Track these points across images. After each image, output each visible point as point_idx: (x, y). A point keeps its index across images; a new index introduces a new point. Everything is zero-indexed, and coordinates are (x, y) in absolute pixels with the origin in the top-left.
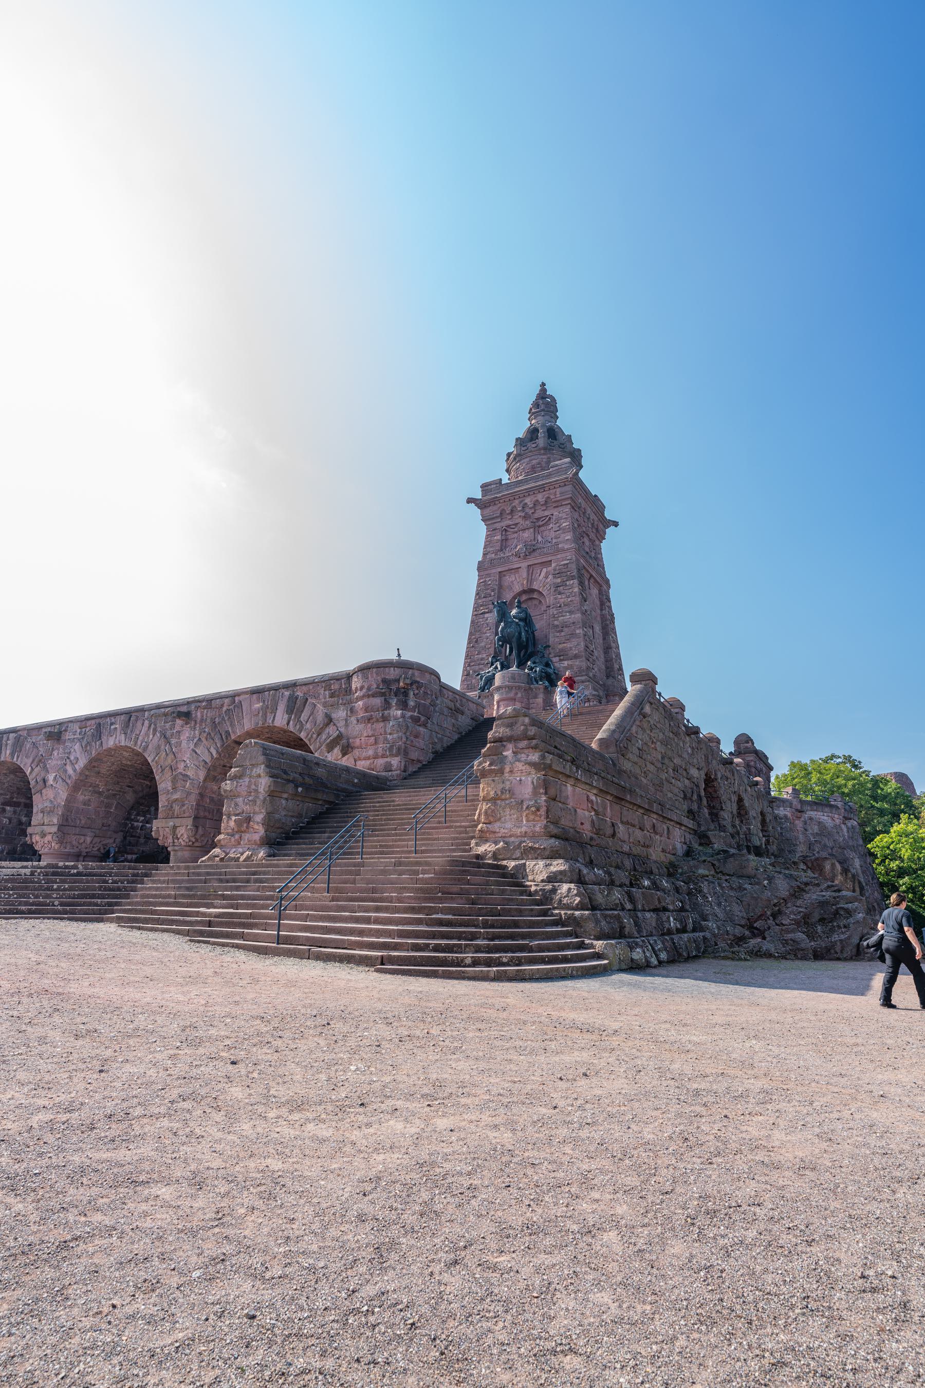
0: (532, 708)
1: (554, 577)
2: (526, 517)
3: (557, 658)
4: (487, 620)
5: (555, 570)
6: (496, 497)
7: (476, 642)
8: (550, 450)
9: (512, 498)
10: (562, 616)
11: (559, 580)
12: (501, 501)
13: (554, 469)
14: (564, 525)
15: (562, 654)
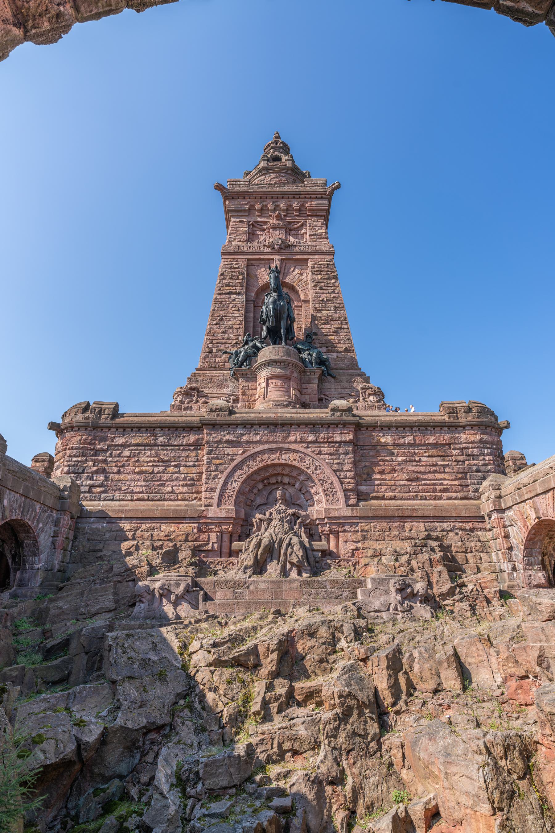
0: (305, 394)
1: (313, 274)
2: (279, 217)
3: (324, 349)
4: (234, 300)
5: (313, 267)
6: (248, 192)
7: (221, 320)
8: (296, 173)
9: (264, 197)
10: (325, 310)
11: (319, 277)
12: (252, 197)
13: (310, 182)
14: (319, 231)
15: (330, 344)
